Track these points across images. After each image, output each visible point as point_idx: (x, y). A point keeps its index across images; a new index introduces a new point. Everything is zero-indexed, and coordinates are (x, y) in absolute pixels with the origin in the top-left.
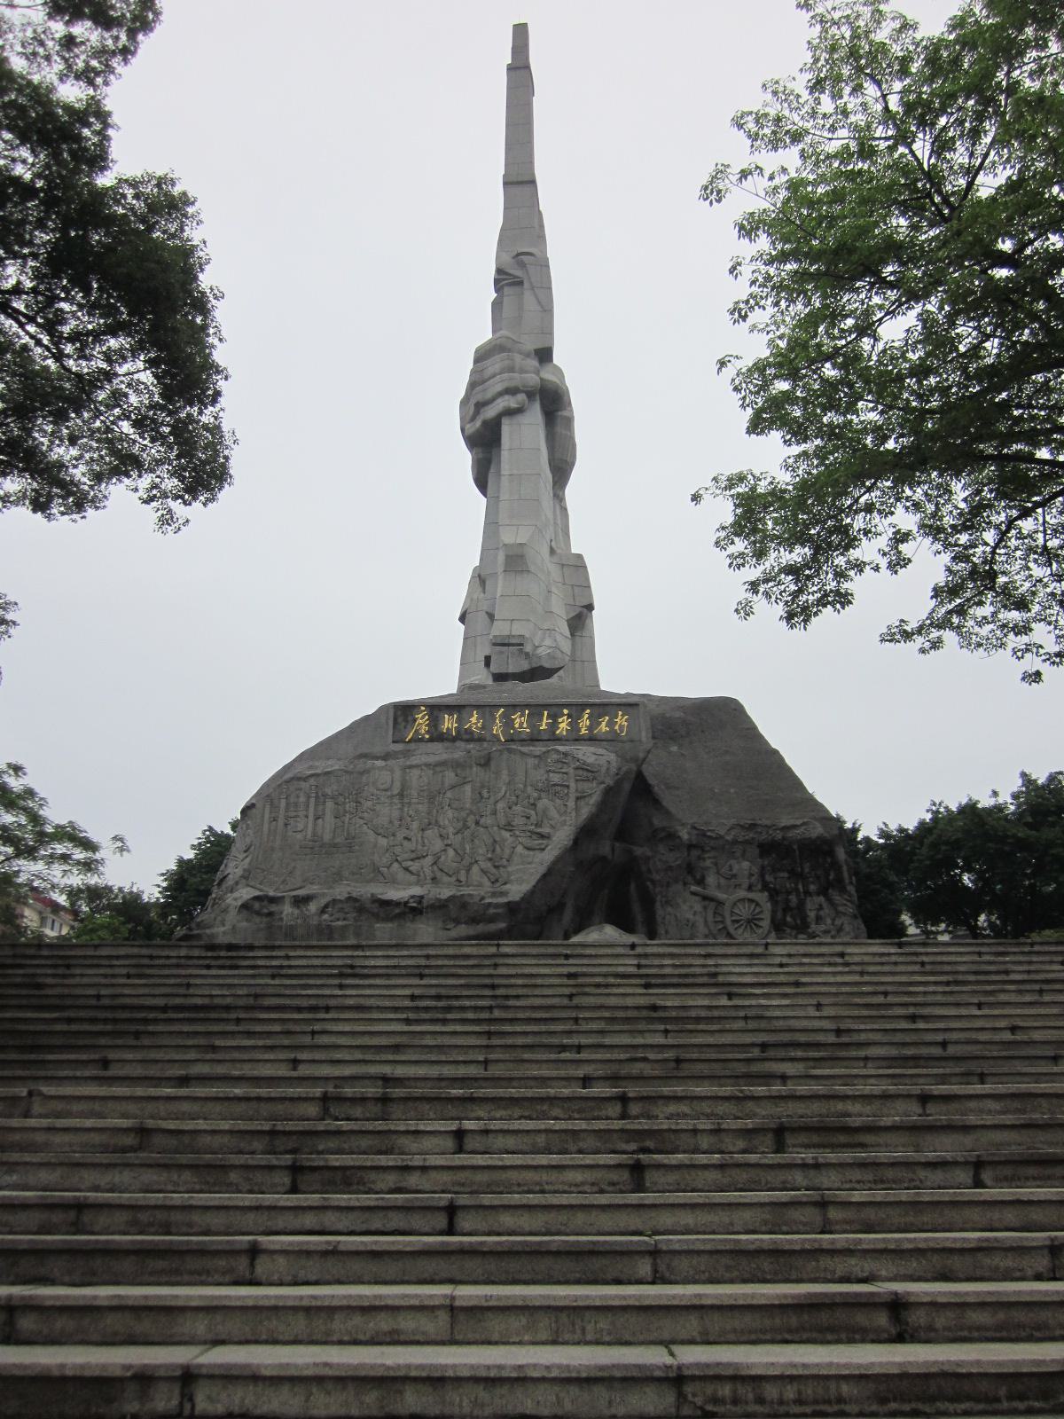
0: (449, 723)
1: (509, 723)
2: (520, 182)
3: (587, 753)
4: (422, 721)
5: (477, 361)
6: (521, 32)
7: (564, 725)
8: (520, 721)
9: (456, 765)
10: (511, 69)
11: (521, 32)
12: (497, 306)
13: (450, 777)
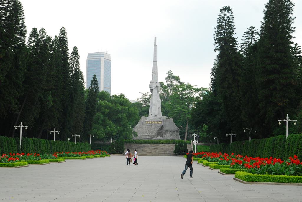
0: (149, 122)
1: (153, 122)
2: (155, 62)
3: (158, 125)
4: (147, 122)
5: (151, 83)
6: (155, 38)
7: (157, 123)
8: (154, 122)
9: (149, 126)
10: (154, 45)
11: (155, 38)
12: (153, 75)
13: (149, 126)
